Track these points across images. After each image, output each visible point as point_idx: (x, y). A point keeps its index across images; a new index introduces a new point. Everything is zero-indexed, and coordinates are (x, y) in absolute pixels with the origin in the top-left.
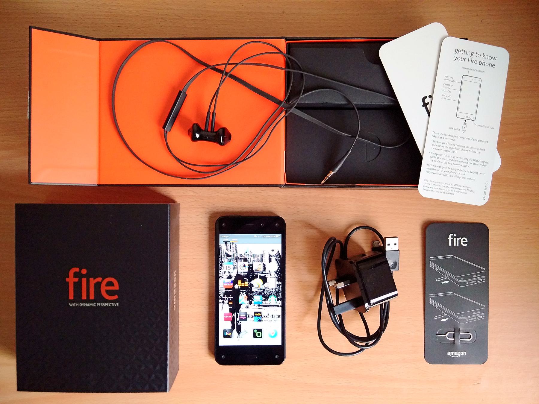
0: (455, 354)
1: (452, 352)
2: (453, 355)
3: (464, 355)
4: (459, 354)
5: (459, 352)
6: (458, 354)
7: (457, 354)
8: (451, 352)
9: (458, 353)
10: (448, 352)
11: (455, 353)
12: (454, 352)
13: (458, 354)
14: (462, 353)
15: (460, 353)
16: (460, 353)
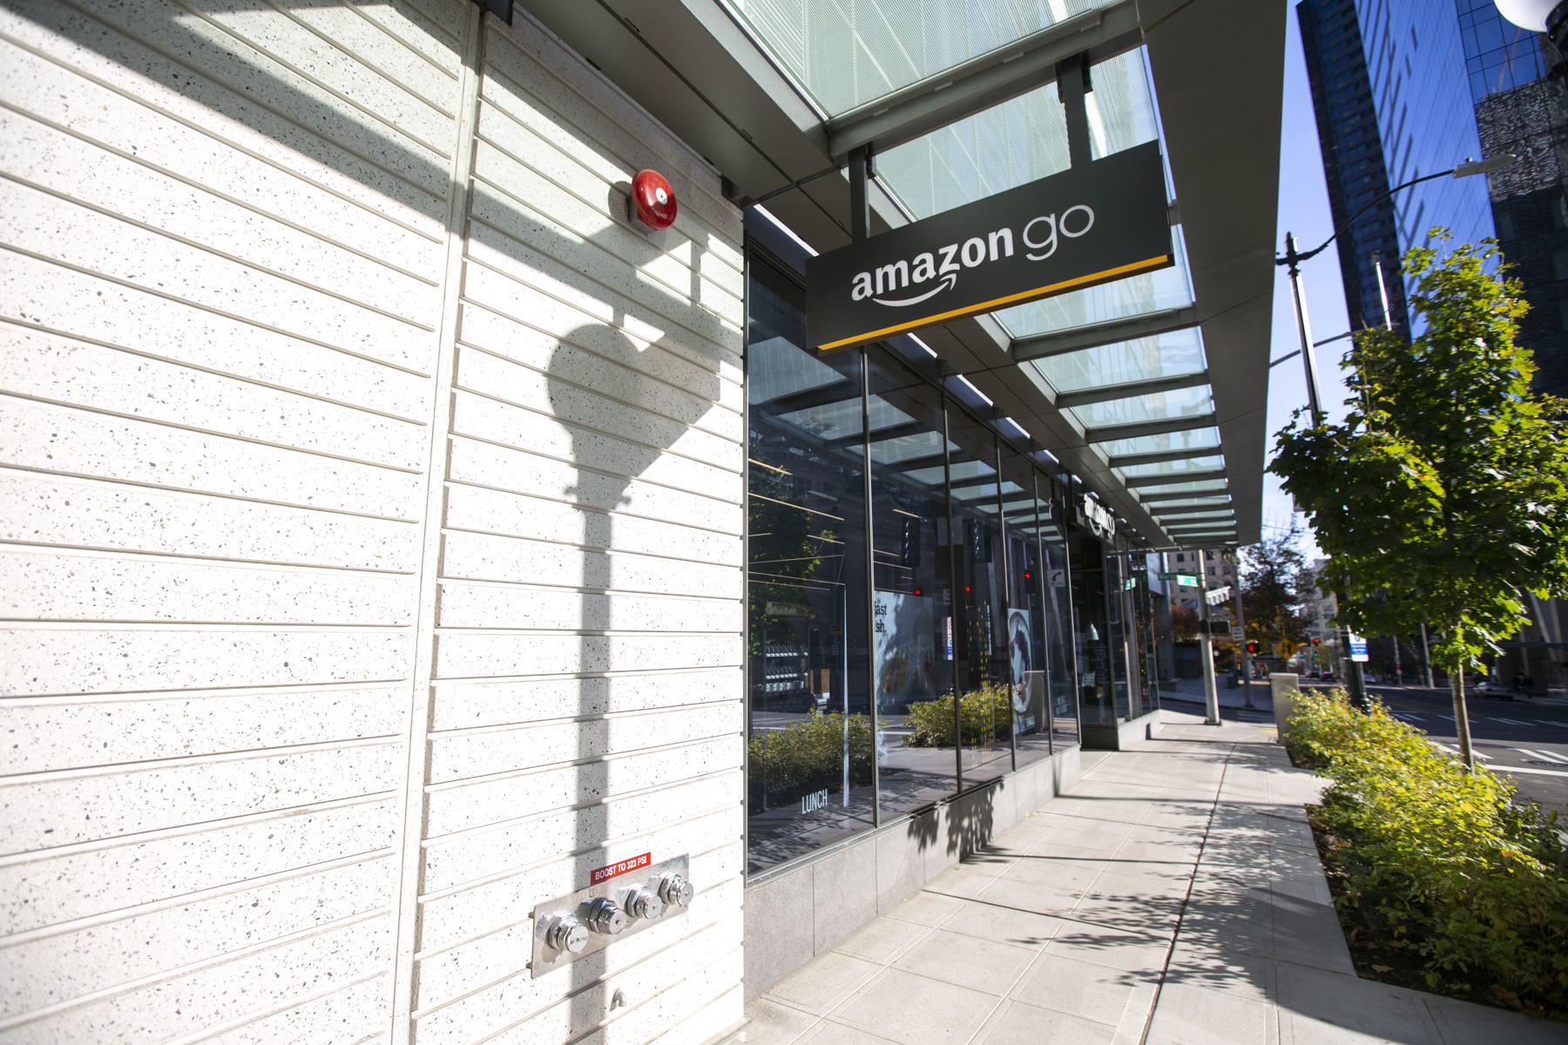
0: (916, 273)
2: (892, 286)
4: (946, 266)
5: (951, 250)
6: (937, 265)
7: (931, 274)
9: (938, 261)
10: (856, 280)
11: (911, 269)
12: (903, 265)
13: (937, 265)
15: (957, 258)
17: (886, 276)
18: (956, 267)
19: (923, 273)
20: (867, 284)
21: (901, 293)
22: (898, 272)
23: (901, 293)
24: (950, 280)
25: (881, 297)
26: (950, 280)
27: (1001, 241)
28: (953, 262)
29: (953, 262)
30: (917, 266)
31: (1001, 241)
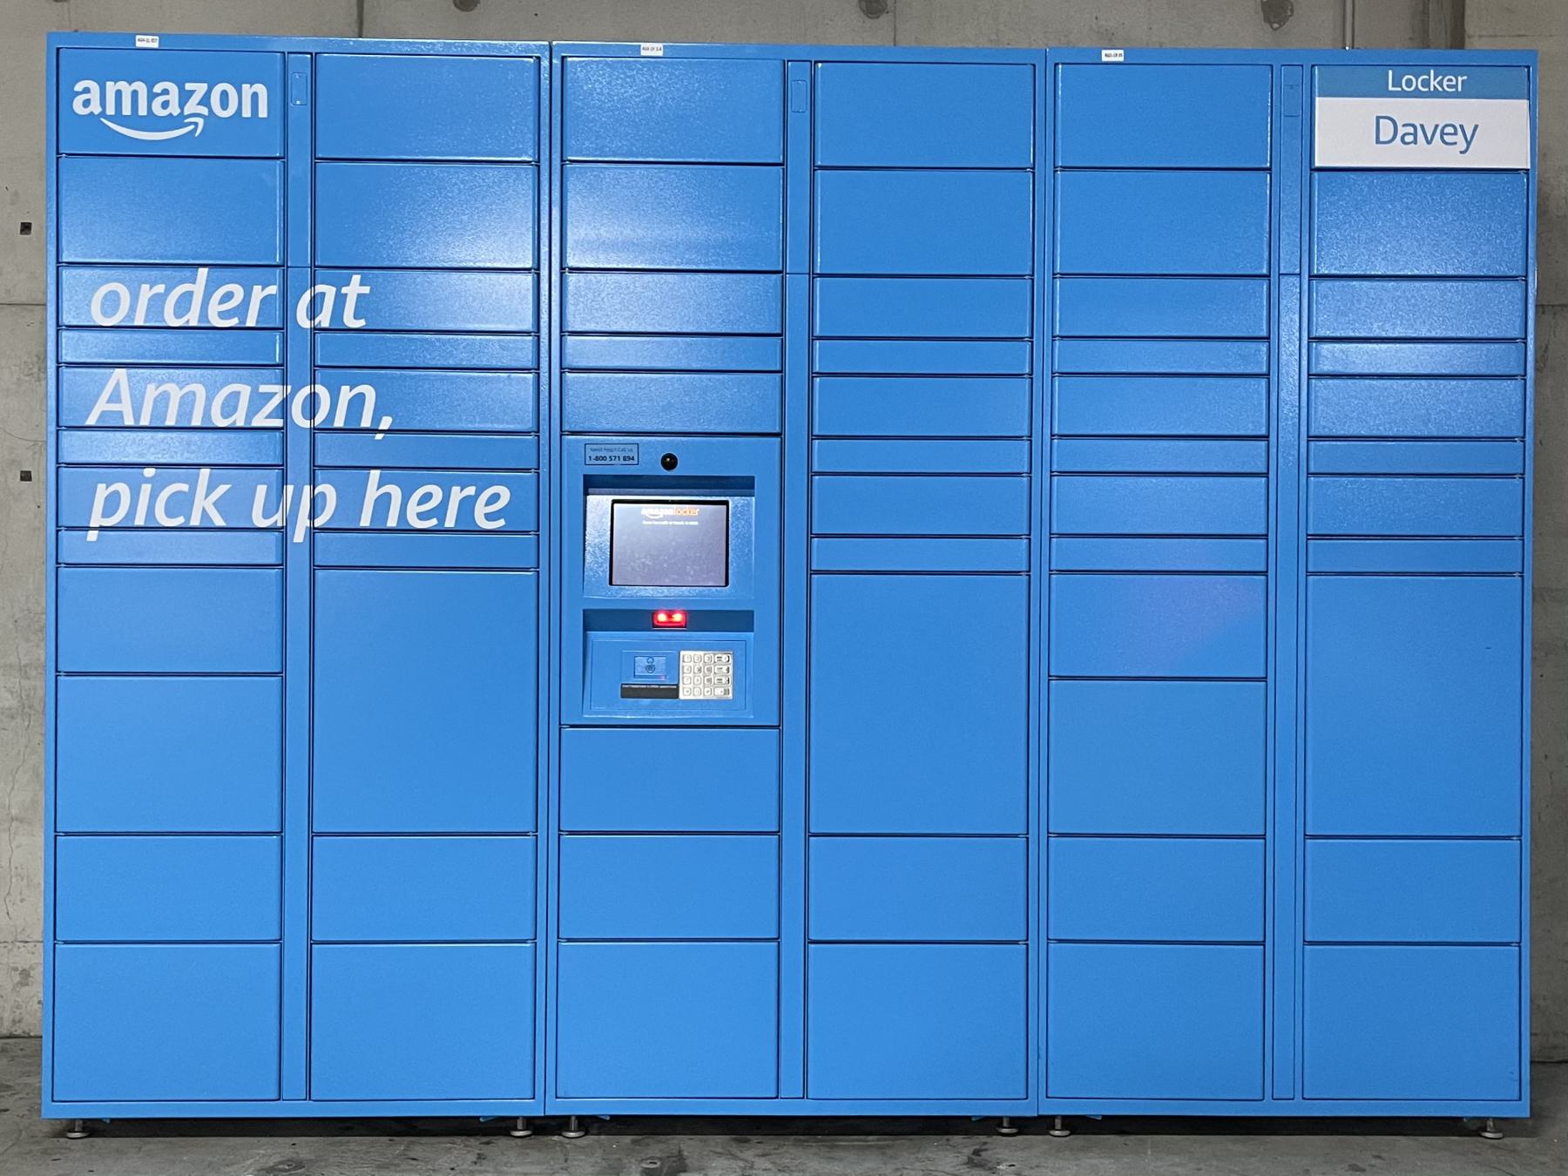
1: (122, 85)
2: (127, 111)
3: (247, 113)
4: (192, 106)
5: (201, 88)
7: (174, 109)
9: (185, 97)
10: (79, 87)
11: (152, 96)
12: (140, 86)
13: (182, 105)
15: (205, 101)
16: (205, 101)
17: (119, 94)
18: (204, 111)
19: (165, 105)
20: (95, 95)
21: (134, 121)
22: (135, 94)
23: (134, 121)
24: (196, 124)
25: (109, 118)
26: (196, 124)
27: (255, 96)
30: (158, 95)
31: (255, 96)
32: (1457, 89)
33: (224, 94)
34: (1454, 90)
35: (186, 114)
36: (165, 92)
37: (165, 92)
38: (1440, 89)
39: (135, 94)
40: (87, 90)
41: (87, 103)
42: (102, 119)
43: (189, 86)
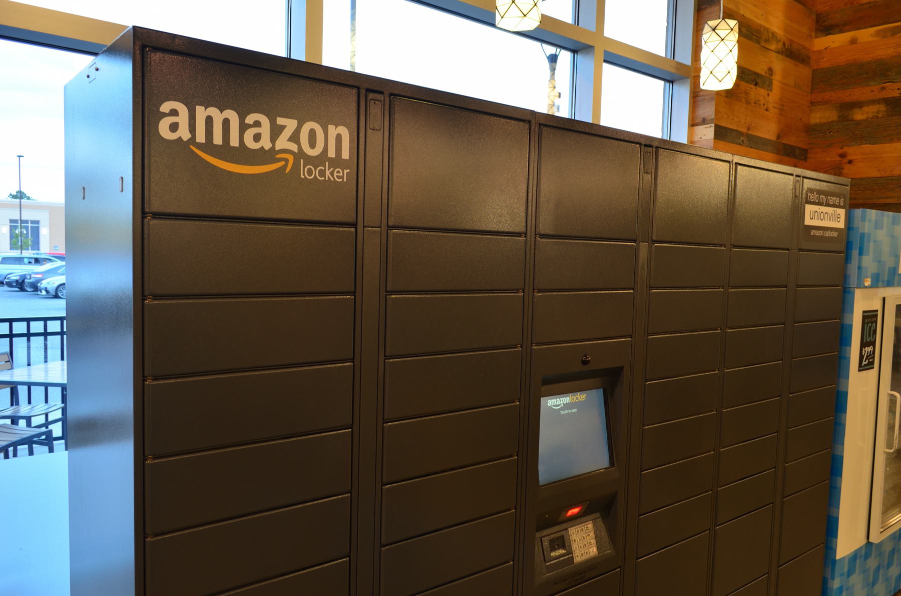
1: (213, 111)
2: (218, 140)
3: (332, 154)
4: (283, 143)
5: (290, 125)
6: (274, 137)
7: (266, 143)
8: (201, 113)
9: (276, 131)
10: (166, 107)
11: (243, 127)
12: (232, 115)
13: (274, 137)
14: (312, 134)
17: (209, 120)
18: (294, 147)
19: (257, 138)
20: (183, 118)
21: (225, 152)
22: (226, 123)
24: (287, 160)
26: (287, 160)
27: (339, 138)
28: (290, 140)
29: (290, 140)
30: (250, 126)
31: (339, 138)
32: (343, 180)
33: (312, 133)
34: (341, 180)
35: (277, 148)
36: (257, 124)
37: (257, 124)
38: (332, 179)
39: (226, 123)
40: (174, 113)
41: (174, 127)
42: (191, 146)
43: (280, 121)
